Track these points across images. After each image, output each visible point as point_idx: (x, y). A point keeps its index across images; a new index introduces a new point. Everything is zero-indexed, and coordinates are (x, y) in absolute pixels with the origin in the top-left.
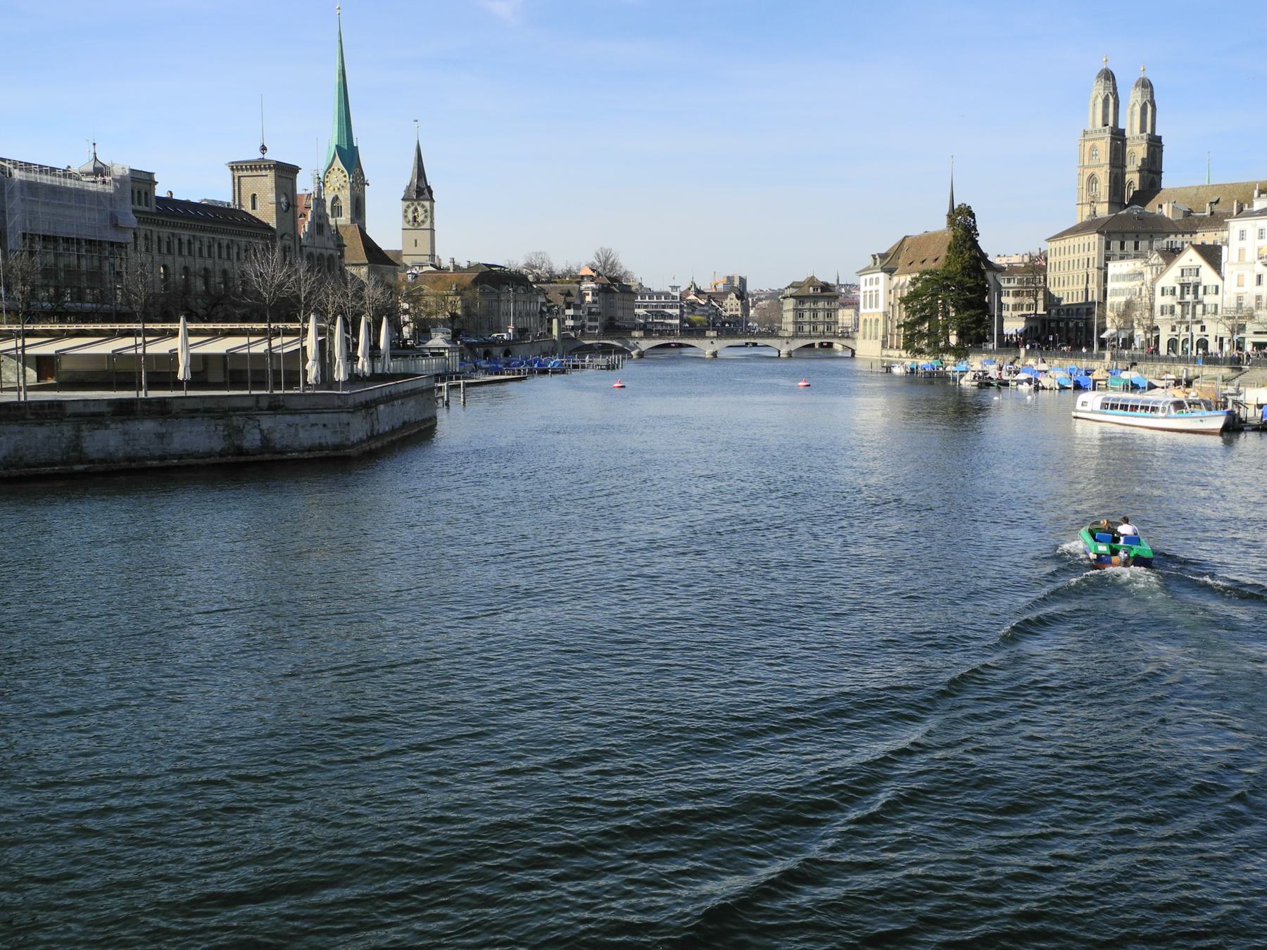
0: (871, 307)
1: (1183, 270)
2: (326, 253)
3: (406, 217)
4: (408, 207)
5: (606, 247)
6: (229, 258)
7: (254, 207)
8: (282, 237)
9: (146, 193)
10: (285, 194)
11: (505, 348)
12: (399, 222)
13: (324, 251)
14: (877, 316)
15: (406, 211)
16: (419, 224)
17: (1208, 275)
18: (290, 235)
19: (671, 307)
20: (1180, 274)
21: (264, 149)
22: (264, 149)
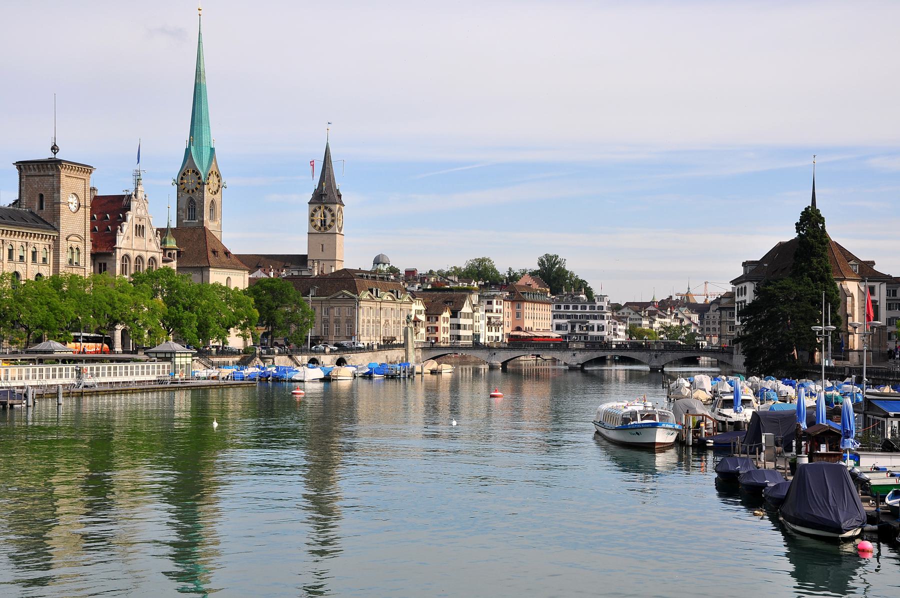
3: (312, 221)
4: (315, 211)
7: (41, 208)
8: (67, 239)
10: (75, 194)
11: (338, 357)
12: (305, 226)
13: (144, 254)
15: (312, 215)
16: (325, 229)
18: (78, 236)
19: (595, 318)
21: (54, 149)
22: (54, 149)
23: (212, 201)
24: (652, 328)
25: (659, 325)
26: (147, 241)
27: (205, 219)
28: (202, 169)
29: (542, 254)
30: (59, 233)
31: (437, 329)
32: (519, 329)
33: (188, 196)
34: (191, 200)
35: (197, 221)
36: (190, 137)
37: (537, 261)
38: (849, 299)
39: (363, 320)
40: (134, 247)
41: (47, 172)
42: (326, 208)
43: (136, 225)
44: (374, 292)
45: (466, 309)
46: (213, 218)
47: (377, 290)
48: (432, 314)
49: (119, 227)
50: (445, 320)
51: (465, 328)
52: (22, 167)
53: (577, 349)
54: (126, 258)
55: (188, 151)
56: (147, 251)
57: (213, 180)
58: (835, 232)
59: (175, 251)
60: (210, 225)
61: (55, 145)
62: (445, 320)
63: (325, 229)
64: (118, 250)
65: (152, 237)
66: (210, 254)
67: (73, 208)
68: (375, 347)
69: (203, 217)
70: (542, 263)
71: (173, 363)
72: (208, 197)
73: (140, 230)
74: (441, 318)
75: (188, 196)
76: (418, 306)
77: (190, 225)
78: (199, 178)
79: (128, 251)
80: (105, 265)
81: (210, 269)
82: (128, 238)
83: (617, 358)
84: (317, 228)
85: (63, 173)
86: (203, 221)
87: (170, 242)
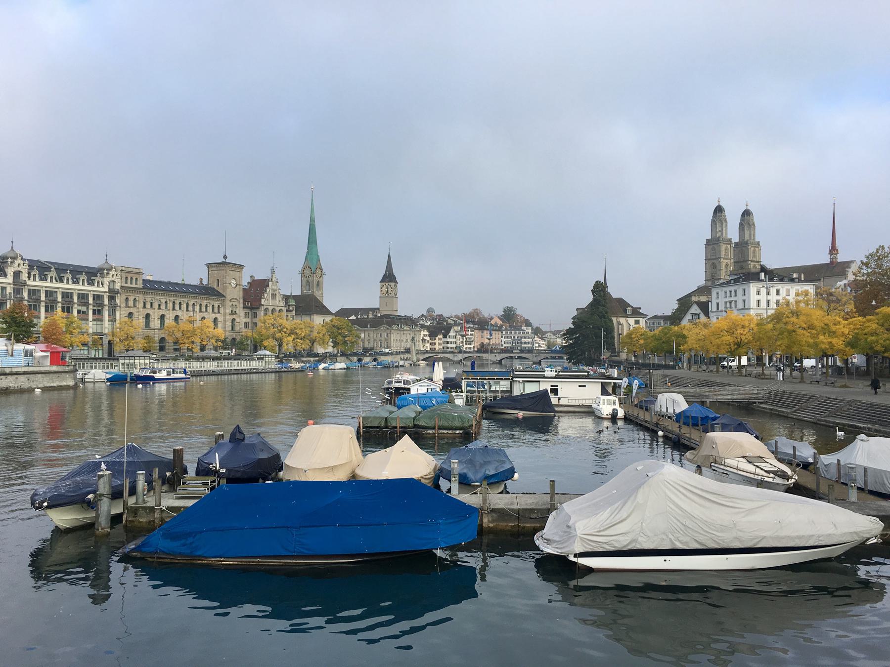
1: (692, 315)
5: (510, 306)
6: (194, 311)
7: (218, 286)
9: (137, 278)
12: (378, 294)
19: (525, 338)
21: (225, 257)
22: (225, 257)
23: (318, 282)
26: (277, 302)
29: (505, 306)
31: (435, 344)
33: (306, 279)
34: (308, 281)
37: (502, 310)
39: (394, 340)
41: (220, 269)
42: (388, 284)
43: (272, 294)
44: (400, 326)
45: (452, 333)
47: (401, 325)
50: (439, 339)
51: (451, 343)
53: (496, 353)
56: (278, 306)
57: (319, 271)
58: (614, 291)
63: (388, 295)
65: (281, 299)
67: (233, 285)
68: (394, 353)
70: (505, 311)
73: (274, 296)
74: (437, 338)
75: (306, 279)
77: (307, 294)
79: (268, 307)
80: (256, 313)
83: (516, 357)
87: (292, 302)
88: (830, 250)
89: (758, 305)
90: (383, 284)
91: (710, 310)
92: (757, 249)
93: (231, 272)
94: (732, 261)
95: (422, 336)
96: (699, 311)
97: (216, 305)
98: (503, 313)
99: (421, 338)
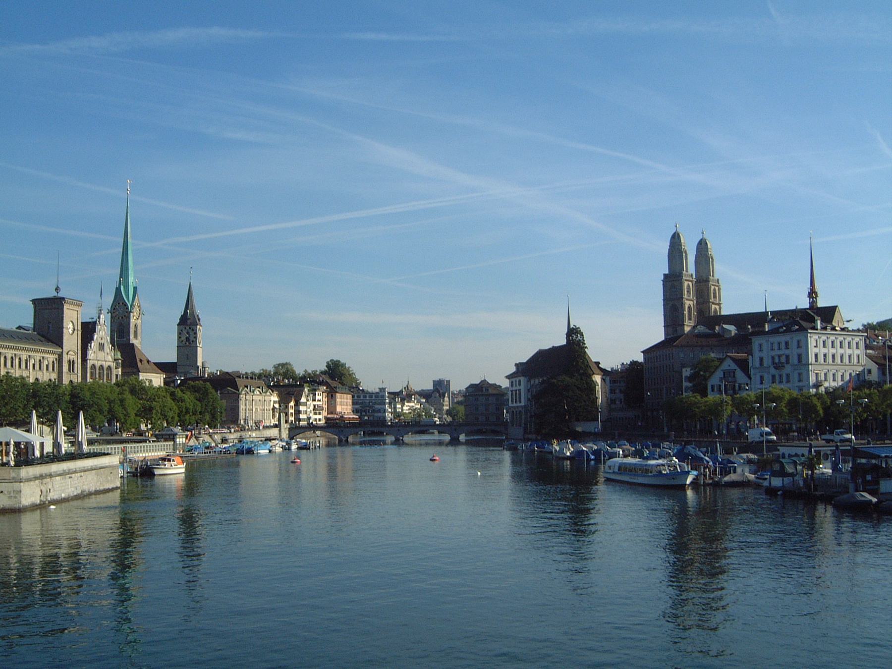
0: (516, 402)
1: (724, 373)
2: (106, 365)
8: (67, 354)
10: (72, 322)
14: (520, 409)
17: (740, 376)
20: (722, 376)
21: (57, 289)
22: (57, 289)
24: (402, 410)
25: (407, 408)
26: (106, 354)
27: (131, 337)
28: (129, 301)
29: (329, 360)
30: (62, 349)
32: (332, 413)
34: (121, 324)
35: (125, 339)
36: (120, 279)
38: (597, 387)
40: (98, 359)
42: (190, 328)
45: (303, 400)
46: (136, 337)
48: (284, 401)
49: (89, 345)
52: (36, 303)
54: (93, 366)
55: (118, 290)
59: (120, 361)
60: (133, 340)
61: (58, 287)
62: (292, 407)
63: (190, 343)
64: (88, 361)
66: (139, 363)
67: (71, 332)
69: (129, 336)
71: (175, 442)
72: (132, 320)
76: (275, 398)
78: (127, 308)
81: (140, 374)
82: (94, 352)
84: (184, 343)
85: (66, 307)
86: (129, 339)
88: (809, 293)
89: (816, 360)
90: (182, 327)
91: (750, 365)
92: (717, 288)
93: (68, 311)
94: (695, 301)
95: (272, 403)
96: (733, 366)
97: (24, 358)
98: (326, 368)
99: (272, 407)
